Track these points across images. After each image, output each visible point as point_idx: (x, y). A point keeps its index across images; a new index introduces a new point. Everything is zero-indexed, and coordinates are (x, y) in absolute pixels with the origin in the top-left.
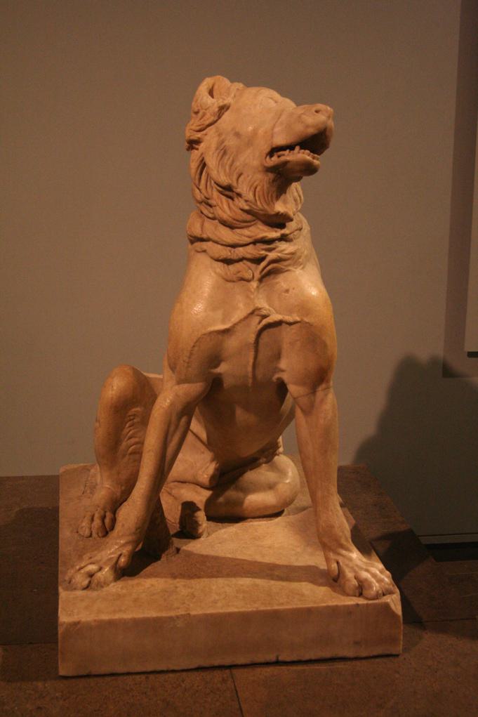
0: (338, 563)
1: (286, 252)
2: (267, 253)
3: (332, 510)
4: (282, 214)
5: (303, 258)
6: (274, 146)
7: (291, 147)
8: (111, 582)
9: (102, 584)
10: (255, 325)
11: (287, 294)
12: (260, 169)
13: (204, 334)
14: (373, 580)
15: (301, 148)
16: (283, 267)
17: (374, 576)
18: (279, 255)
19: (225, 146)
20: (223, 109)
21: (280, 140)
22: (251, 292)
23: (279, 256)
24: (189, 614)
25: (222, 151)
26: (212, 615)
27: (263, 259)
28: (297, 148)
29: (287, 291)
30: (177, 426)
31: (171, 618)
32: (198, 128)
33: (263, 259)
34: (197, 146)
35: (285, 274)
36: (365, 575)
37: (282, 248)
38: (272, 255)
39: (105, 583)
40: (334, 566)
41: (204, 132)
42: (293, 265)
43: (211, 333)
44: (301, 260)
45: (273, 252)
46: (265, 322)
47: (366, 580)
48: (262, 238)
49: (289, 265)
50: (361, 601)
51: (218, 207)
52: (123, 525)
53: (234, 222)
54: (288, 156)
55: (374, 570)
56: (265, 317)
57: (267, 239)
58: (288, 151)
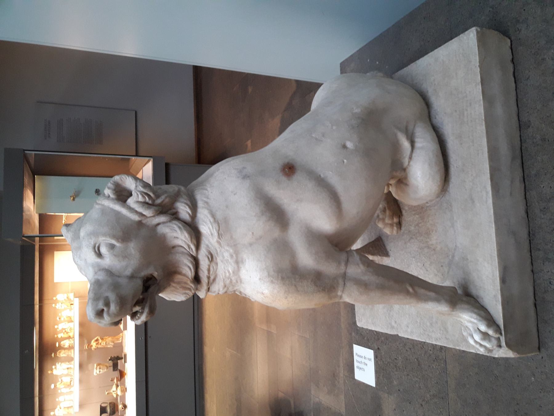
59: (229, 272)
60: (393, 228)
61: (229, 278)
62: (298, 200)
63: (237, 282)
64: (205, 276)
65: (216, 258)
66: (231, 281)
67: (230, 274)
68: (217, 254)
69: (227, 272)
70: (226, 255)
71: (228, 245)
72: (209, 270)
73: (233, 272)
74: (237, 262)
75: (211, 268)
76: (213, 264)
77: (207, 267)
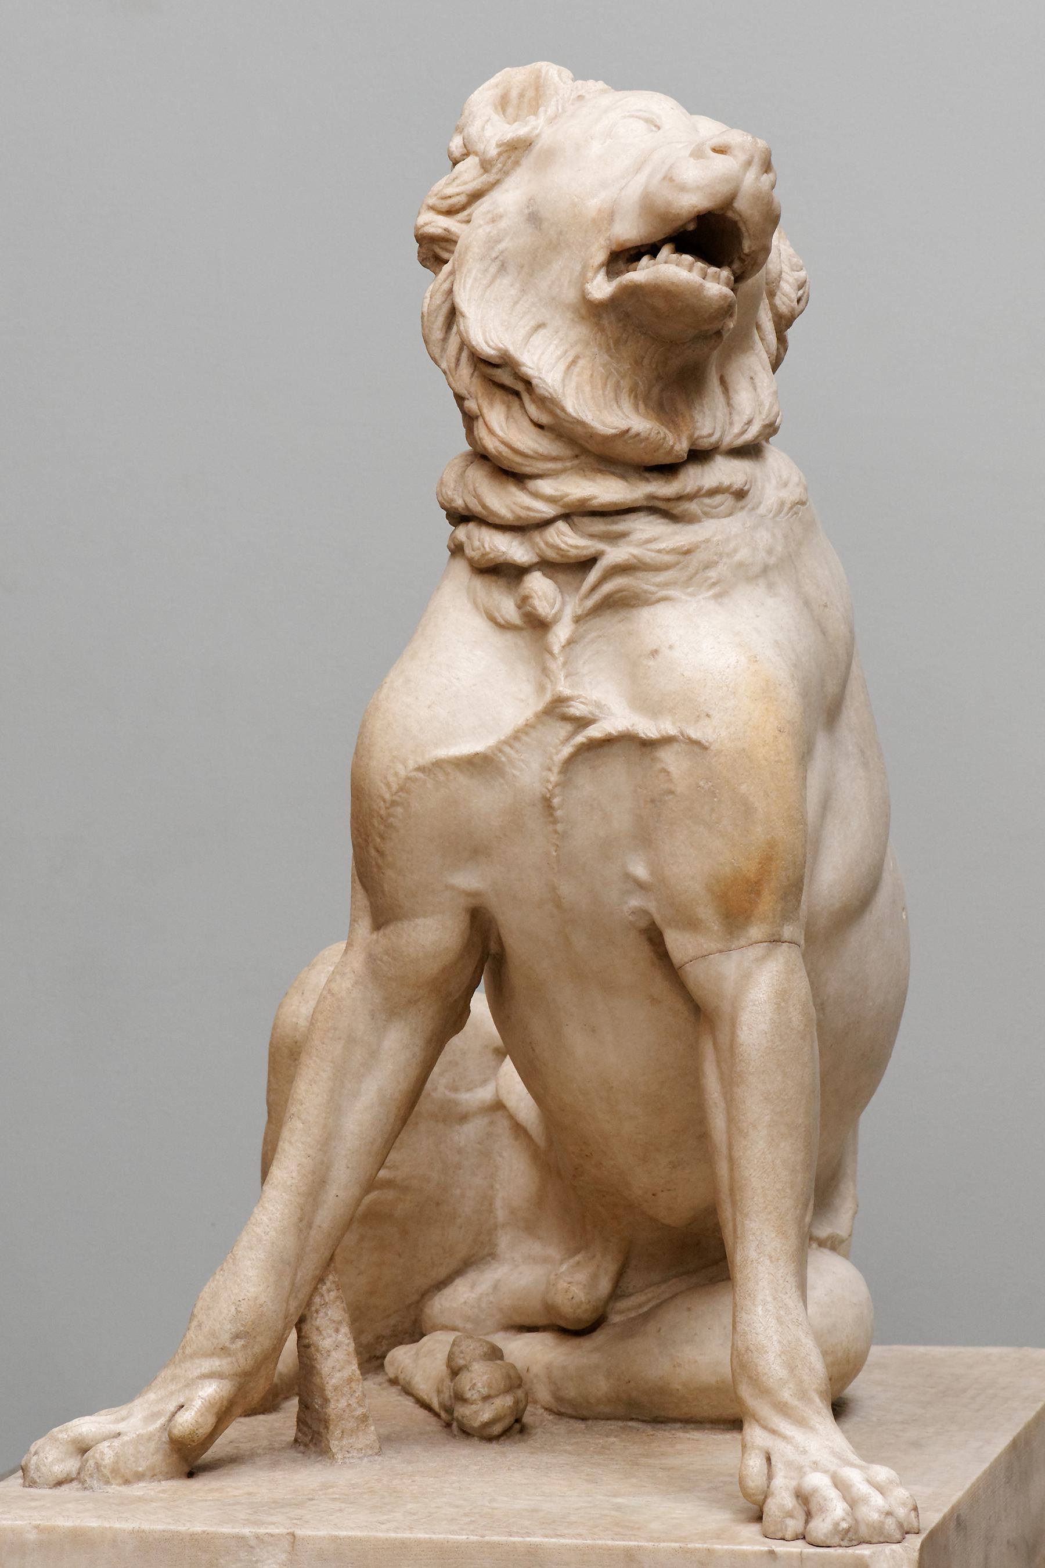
0: (769, 1459)
1: (663, 546)
2: (601, 546)
3: (765, 1303)
4: (638, 435)
5: (722, 568)
6: (614, 247)
7: (653, 250)
8: (139, 1477)
9: (106, 1471)
10: (560, 744)
11: (651, 663)
12: (583, 311)
13: (421, 769)
14: (833, 1493)
15: (680, 249)
16: (653, 589)
17: (840, 1485)
18: (636, 551)
19: (502, 252)
20: (516, 150)
21: (629, 230)
22: (551, 653)
23: (634, 556)
24: (293, 1535)
25: (498, 263)
26: (354, 1541)
27: (587, 563)
28: (665, 252)
29: (655, 653)
30: (373, 1054)
31: (241, 1539)
32: (445, 204)
33: (587, 563)
34: (445, 255)
35: (660, 610)
36: (818, 1481)
37: (646, 535)
38: (614, 554)
39: (115, 1471)
40: (755, 1464)
41: (465, 213)
42: (689, 581)
43: (438, 764)
44: (713, 574)
45: (622, 542)
46: (580, 739)
47: (815, 1491)
48: (583, 502)
49: (666, 585)
50: (798, 1547)
51: (480, 420)
52: (200, 1325)
53: (518, 459)
54: (644, 272)
55: (854, 1476)
56: (582, 723)
57: (595, 502)
58: (645, 260)
59: (735, 551)
60: (509, 1390)
61: (721, 555)
62: (862, 751)
63: (714, 584)
64: (699, 483)
65: (742, 508)
66: (708, 566)
67: (729, 555)
68: (753, 509)
69: (732, 545)
70: (764, 537)
71: (786, 537)
72: (713, 492)
73: (740, 565)
74: (765, 570)
75: (718, 499)
76: (728, 501)
77: (726, 482)
